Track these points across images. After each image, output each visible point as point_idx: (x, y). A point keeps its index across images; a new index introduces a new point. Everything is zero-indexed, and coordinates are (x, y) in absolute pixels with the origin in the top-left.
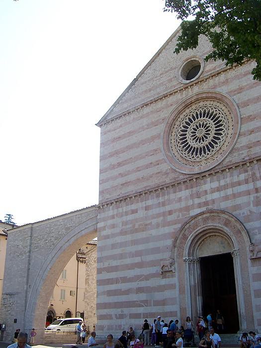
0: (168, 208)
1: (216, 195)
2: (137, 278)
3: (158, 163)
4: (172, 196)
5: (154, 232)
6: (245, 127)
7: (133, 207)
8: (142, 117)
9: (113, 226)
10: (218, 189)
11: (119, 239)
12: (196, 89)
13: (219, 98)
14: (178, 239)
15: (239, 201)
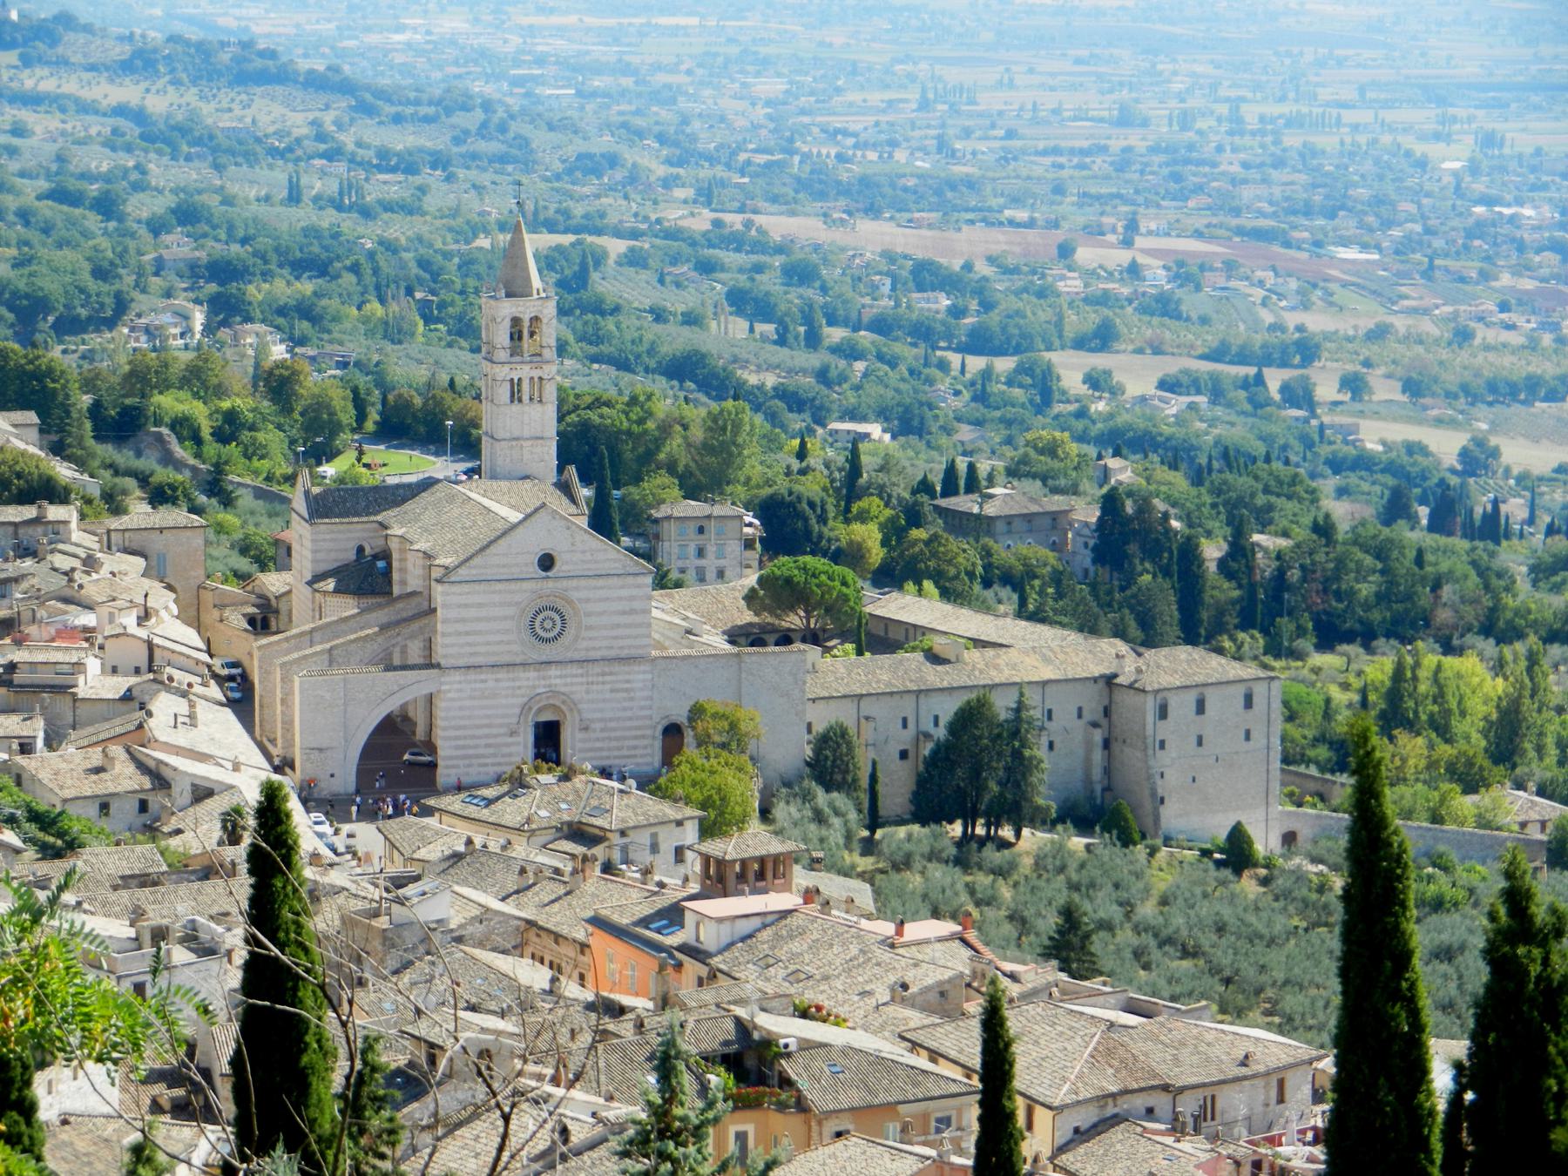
0: (517, 684)
1: (558, 681)
2: (487, 736)
3: (508, 643)
4: (522, 675)
5: (504, 701)
6: (584, 634)
7: (483, 677)
8: (494, 592)
9: (460, 690)
10: (561, 677)
11: (468, 703)
12: (551, 584)
13: (570, 602)
14: (525, 708)
15: (574, 688)
